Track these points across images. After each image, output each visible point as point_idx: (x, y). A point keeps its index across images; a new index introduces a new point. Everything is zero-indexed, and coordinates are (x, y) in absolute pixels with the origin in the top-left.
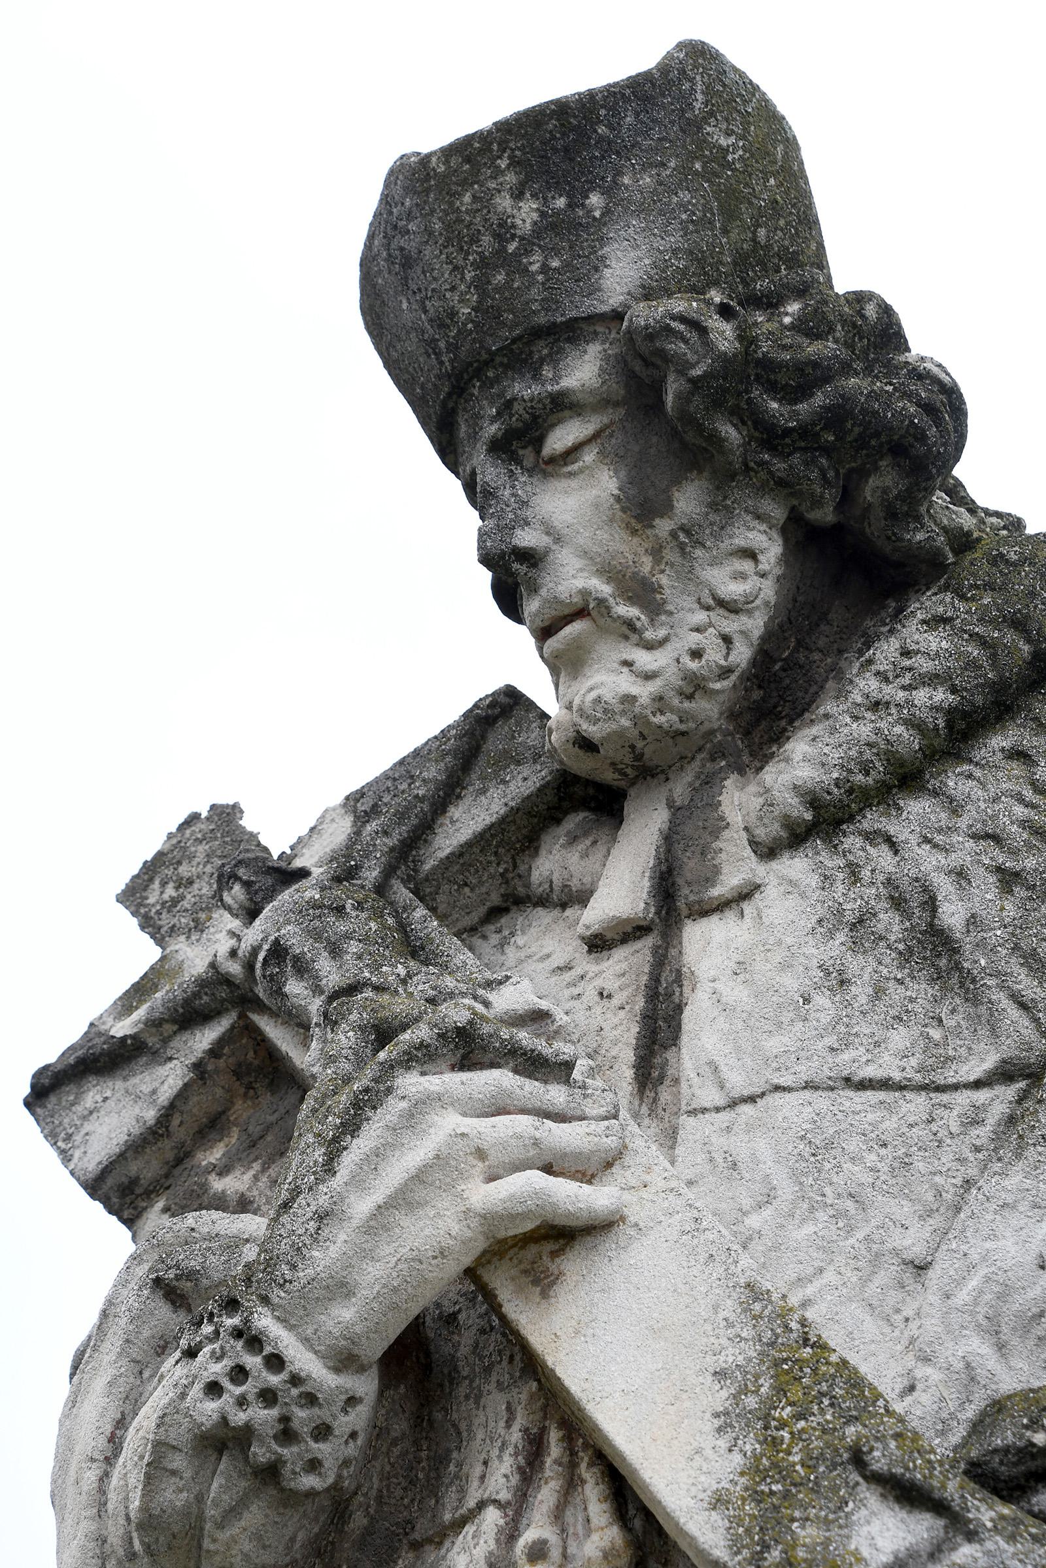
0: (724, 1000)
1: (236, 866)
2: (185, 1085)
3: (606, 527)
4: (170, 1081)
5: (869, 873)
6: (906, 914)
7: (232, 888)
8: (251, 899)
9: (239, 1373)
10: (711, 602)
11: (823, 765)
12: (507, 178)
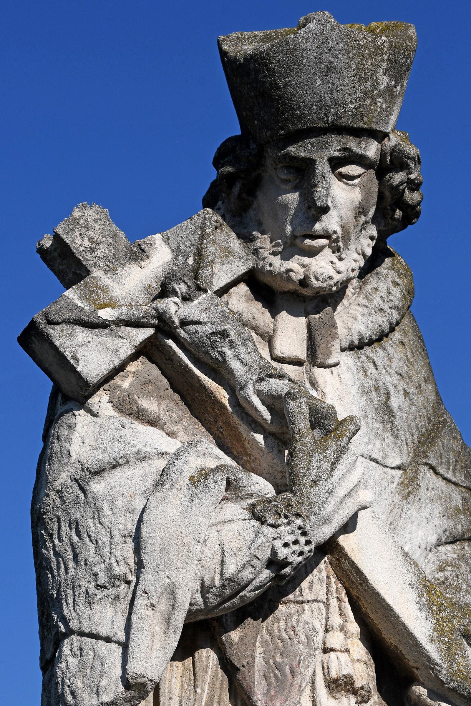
3: (351, 211)
6: (379, 395)
7: (180, 284)
8: (189, 294)
9: (296, 542)
11: (367, 327)
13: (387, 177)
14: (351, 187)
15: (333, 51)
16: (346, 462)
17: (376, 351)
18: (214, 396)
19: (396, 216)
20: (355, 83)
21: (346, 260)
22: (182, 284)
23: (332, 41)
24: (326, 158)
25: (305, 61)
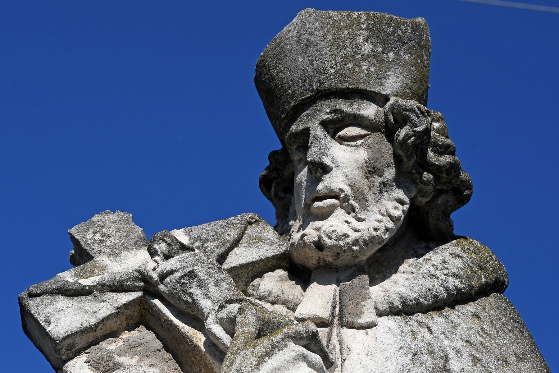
0: (363, 363)
1: (164, 236)
2: (111, 315)
4: (105, 310)
5: (420, 337)
7: (160, 244)
8: (169, 251)
10: (385, 214)
11: (411, 290)
12: (364, 32)
13: (396, 136)
14: (353, 148)
15: (310, 30)
16: (281, 358)
17: (432, 318)
18: (191, 341)
19: (425, 179)
20: (334, 51)
21: (367, 220)
22: (162, 243)
23: (309, 24)
24: (318, 122)
25: (288, 47)
